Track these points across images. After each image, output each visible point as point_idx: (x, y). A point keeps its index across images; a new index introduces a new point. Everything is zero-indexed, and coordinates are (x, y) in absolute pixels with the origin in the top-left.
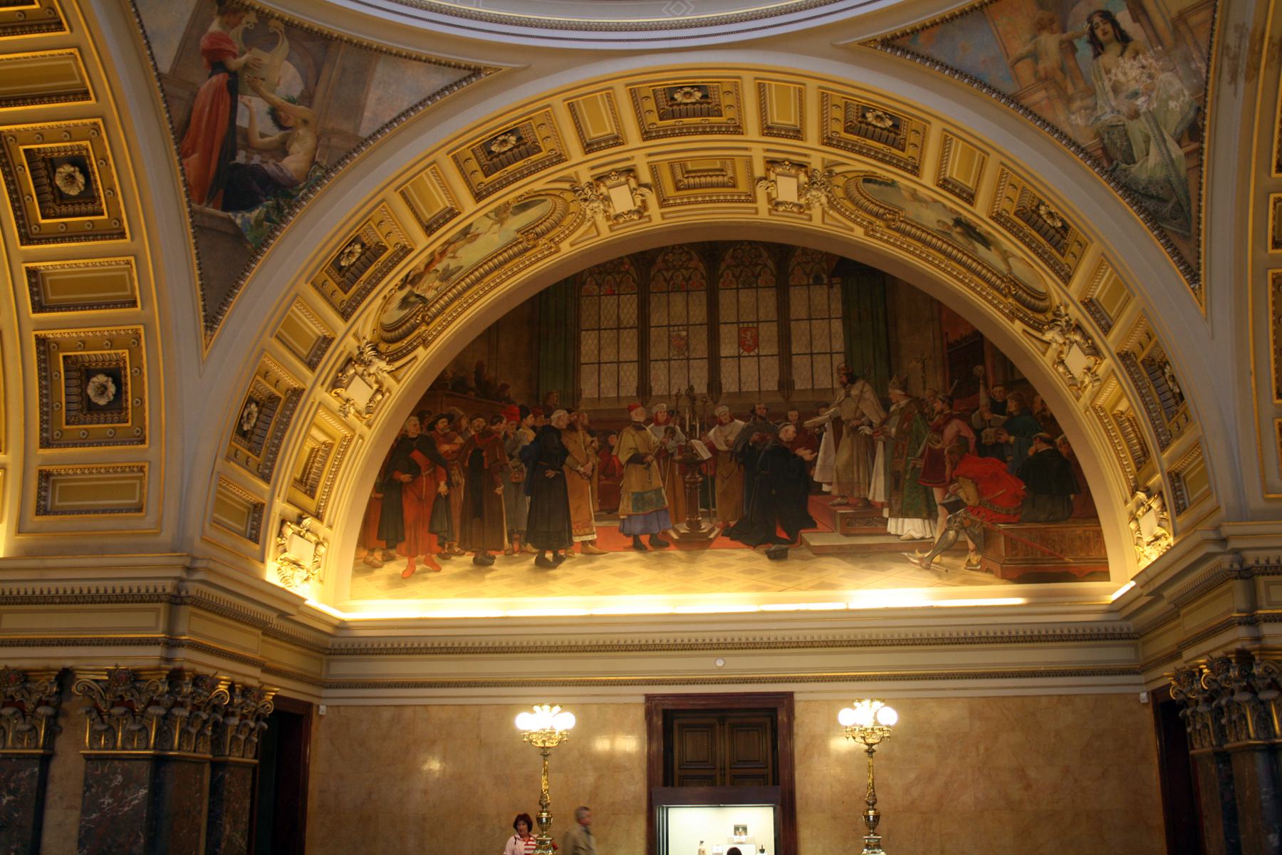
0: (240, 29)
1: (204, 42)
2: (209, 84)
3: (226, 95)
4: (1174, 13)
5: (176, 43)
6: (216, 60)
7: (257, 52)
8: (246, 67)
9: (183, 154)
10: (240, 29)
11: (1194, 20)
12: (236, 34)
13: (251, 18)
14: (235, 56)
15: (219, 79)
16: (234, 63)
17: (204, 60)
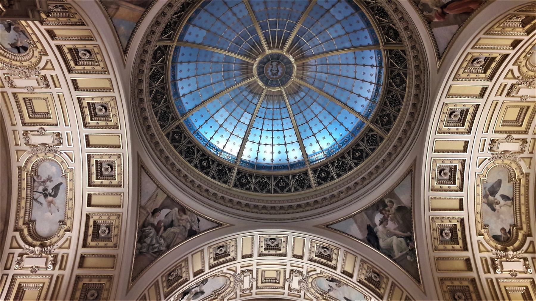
0: (430, 14)
1: (442, 20)
2: (451, 13)
3: (448, 6)
4: (120, 8)
5: (449, 27)
6: (443, 15)
7: (431, 6)
8: (437, 6)
9: (473, 10)
10: (430, 14)
11: (114, 11)
12: (432, 14)
13: (425, 13)
14: (437, 11)
15: (446, 11)
16: (440, 10)
17: (446, 17)
